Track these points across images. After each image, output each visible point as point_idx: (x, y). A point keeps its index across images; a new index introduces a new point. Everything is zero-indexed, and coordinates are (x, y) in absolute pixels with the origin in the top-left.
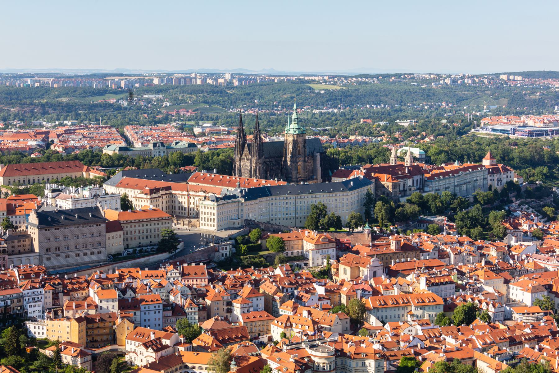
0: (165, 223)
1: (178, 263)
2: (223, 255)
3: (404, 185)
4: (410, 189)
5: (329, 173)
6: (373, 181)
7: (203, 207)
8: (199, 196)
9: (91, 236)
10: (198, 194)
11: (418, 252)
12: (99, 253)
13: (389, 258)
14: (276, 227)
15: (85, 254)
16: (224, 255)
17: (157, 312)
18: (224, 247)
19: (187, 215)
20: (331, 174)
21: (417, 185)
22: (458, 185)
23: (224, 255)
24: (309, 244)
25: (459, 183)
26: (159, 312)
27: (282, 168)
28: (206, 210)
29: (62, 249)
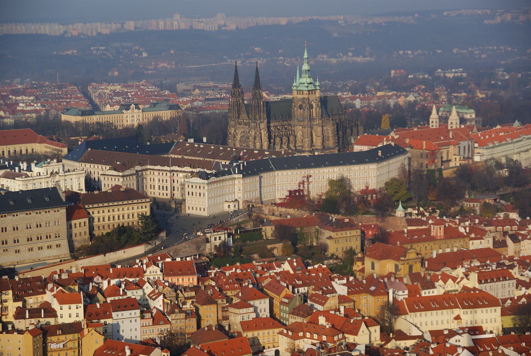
0: (142, 207)
1: (159, 258)
8: (185, 172)
9: (48, 224)
11: (467, 240)
12: (58, 246)
13: (429, 247)
15: (40, 248)
17: (133, 320)
20: (353, 141)
21: (464, 153)
22: (519, 153)
26: (136, 321)
28: (194, 190)
29: (10, 242)
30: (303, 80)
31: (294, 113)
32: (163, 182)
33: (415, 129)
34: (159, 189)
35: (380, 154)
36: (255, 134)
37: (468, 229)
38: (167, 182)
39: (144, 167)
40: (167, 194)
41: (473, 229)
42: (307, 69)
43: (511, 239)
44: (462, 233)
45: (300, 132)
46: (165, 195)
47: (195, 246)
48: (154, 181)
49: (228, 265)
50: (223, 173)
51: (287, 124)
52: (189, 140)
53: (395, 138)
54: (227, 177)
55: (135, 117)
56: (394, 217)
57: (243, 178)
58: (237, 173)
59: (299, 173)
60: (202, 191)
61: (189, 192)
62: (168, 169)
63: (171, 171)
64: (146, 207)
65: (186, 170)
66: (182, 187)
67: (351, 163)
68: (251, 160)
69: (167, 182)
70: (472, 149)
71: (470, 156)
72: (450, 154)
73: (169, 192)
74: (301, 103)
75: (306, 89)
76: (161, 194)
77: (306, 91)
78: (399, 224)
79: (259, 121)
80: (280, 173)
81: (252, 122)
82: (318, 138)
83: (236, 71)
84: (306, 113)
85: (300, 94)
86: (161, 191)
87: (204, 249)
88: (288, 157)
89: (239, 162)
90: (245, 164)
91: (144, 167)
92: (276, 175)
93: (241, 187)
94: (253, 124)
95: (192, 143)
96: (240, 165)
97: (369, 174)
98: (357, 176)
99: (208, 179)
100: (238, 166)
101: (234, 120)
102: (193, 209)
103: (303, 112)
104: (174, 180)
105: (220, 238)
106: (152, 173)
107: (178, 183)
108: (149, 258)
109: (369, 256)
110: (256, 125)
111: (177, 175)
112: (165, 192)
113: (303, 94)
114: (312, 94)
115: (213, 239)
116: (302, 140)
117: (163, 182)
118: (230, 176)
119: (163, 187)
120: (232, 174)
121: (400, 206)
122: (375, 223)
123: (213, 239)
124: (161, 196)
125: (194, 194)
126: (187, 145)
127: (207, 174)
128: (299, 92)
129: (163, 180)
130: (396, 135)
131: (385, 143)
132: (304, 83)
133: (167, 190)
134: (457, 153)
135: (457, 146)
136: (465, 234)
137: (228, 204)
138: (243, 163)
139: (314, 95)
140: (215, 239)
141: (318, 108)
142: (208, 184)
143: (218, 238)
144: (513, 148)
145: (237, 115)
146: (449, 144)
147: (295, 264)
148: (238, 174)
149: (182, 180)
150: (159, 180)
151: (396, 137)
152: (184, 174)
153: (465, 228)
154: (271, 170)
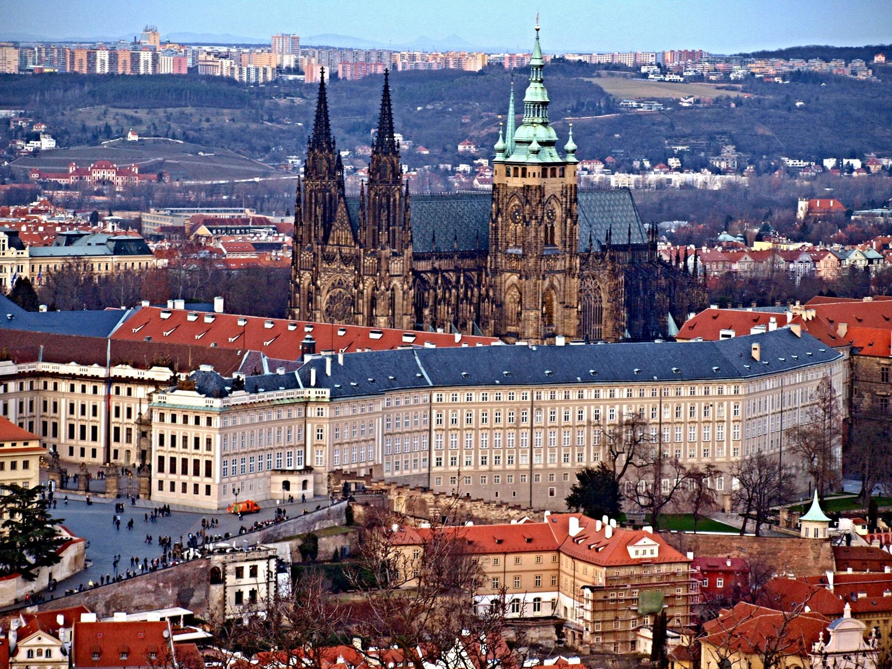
0: (14, 466)
2: (239, 595)
5: (666, 327)
6: (845, 354)
7: (168, 418)
8: (151, 382)
10: (147, 375)
14: (455, 504)
16: (246, 596)
18: (247, 567)
19: (100, 458)
23: (246, 596)
24: (580, 565)
27: (481, 298)
30: (523, 133)
31: (496, 234)
32: (83, 413)
34: (72, 436)
36: (375, 288)
38: (95, 414)
39: (27, 368)
40: (94, 452)
42: (540, 99)
45: (514, 292)
46: (88, 453)
47: (176, 590)
48: (55, 411)
50: (273, 384)
51: (473, 266)
52: (170, 304)
53: (804, 318)
54: (283, 394)
55: (8, 270)
56: (796, 540)
57: (331, 399)
58: (313, 383)
59: (505, 397)
60: (203, 433)
61: (162, 437)
62: (101, 372)
63: (109, 381)
64: (26, 465)
65: (157, 378)
66: (144, 429)
68: (359, 351)
69: (95, 414)
73: (101, 443)
74: (517, 202)
75: (534, 159)
76: (77, 452)
77: (533, 164)
78: (811, 563)
79: (388, 251)
82: (567, 311)
83: (322, 99)
84: (533, 234)
85: (516, 176)
86: (77, 443)
89: (323, 353)
90: (341, 361)
91: (27, 368)
92: (434, 400)
93: (326, 428)
94: (368, 261)
95: (179, 312)
96: (323, 361)
98: (682, 415)
99: (222, 394)
100: (320, 365)
101: (311, 249)
102: (173, 489)
103: (526, 232)
104: (117, 409)
105: (254, 572)
106: (50, 386)
107: (129, 416)
108: (28, 618)
109: (715, 642)
110: (379, 259)
111: (129, 392)
112: (88, 444)
114: (553, 175)
115: (230, 568)
116: (519, 314)
117: (83, 413)
118: (294, 393)
119: (83, 428)
120: (299, 387)
121: (816, 508)
122: (734, 554)
124: (77, 458)
125: (179, 441)
127: (226, 384)
128: (512, 168)
129: (83, 407)
130: (806, 309)
132: (530, 143)
133: (94, 438)
137: (282, 478)
138: (334, 359)
141: (569, 221)
142: (224, 412)
143: (247, 572)
145: (321, 233)
148: (316, 386)
149: (145, 408)
150: (72, 406)
151: (810, 314)
152: (152, 389)
154: (419, 384)
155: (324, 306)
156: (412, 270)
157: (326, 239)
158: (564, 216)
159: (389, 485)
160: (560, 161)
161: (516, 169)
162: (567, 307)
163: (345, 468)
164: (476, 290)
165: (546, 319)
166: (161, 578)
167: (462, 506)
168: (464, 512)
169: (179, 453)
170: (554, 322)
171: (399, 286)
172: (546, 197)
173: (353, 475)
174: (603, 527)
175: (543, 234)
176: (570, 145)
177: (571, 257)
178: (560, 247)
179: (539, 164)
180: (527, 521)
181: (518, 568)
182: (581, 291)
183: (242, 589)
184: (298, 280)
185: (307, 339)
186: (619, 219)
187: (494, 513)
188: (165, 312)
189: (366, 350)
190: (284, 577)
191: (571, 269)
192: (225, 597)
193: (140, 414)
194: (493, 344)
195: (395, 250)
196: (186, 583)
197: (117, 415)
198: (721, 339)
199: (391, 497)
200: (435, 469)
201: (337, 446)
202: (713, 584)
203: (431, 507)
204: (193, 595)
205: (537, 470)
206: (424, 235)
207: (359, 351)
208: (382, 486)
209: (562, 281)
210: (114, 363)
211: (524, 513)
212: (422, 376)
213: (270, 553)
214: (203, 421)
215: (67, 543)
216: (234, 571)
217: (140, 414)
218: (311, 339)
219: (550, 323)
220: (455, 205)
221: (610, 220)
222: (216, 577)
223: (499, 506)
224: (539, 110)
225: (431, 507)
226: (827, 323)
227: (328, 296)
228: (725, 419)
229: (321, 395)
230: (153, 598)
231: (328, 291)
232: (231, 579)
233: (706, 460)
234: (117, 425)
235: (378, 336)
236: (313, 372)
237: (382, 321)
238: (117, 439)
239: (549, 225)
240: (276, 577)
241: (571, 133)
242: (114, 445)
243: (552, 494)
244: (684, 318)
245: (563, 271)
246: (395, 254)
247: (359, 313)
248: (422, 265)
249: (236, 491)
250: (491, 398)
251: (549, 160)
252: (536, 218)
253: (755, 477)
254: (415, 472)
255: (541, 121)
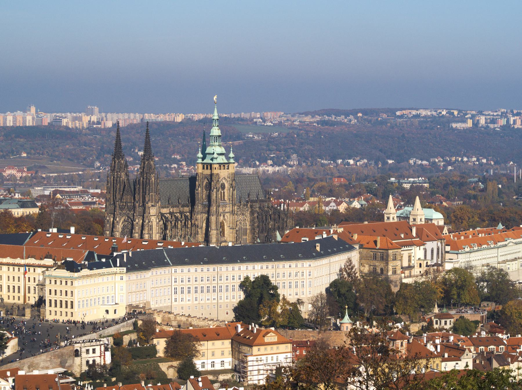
3: (410, 257)
4: (420, 264)
5: (276, 237)
11: (438, 361)
14: (184, 319)
20: (279, 238)
21: (432, 258)
22: (504, 262)
25: (504, 258)
31: (198, 196)
33: (366, 223)
35: (318, 249)
37: (439, 347)
40: (19, 297)
41: (446, 347)
42: (217, 134)
43: (497, 361)
44: (432, 353)
46: (16, 298)
47: (59, 360)
49: (105, 386)
50: (100, 266)
52: (51, 230)
53: (338, 231)
57: (127, 272)
58: (118, 265)
61: (50, 290)
63: (25, 266)
67: (278, 259)
68: (139, 250)
69: (19, 281)
70: (442, 254)
71: (440, 262)
72: (412, 258)
76: (11, 298)
79: (150, 204)
80: (179, 269)
81: (139, 206)
86: (11, 294)
87: (71, 366)
88: (190, 249)
90: (130, 255)
96: (122, 255)
97: (303, 275)
104: (29, 278)
105: (94, 351)
111: (34, 271)
112: (16, 294)
113: (211, 169)
115: (84, 350)
120: (111, 267)
123: (84, 350)
125: (58, 293)
126: (49, 235)
130: (339, 228)
131: (325, 236)
133: (19, 292)
134: (422, 257)
135: (422, 247)
136: (435, 353)
138: (128, 254)
139: (226, 170)
140: (88, 351)
143: (91, 351)
144: (496, 255)
146: (412, 244)
147: (201, 384)
149: (41, 278)
151: (340, 230)
153: (436, 348)
154: (165, 264)
155: (120, 230)
156: (160, 213)
157: (121, 199)
158: (229, 187)
159: (154, 310)
160: (227, 162)
161: (207, 166)
162: (231, 228)
163: (133, 303)
164: (189, 221)
165: (222, 234)
166: (52, 354)
167: (187, 320)
168: (187, 322)
169: (58, 298)
170: (225, 236)
171: (155, 220)
172: (221, 179)
173: (137, 307)
174: (252, 328)
175: (220, 196)
176: (232, 155)
177: (233, 205)
178: (228, 201)
179: (218, 164)
180: (217, 326)
181: (213, 347)
182: (237, 221)
183: (89, 359)
184: (108, 218)
185: (114, 245)
186: (253, 188)
187: (202, 323)
188: (49, 234)
189: (142, 250)
190: (108, 354)
191: (232, 211)
192: (81, 363)
193: (39, 280)
194: (200, 246)
195: (153, 204)
196: (64, 357)
197: (29, 281)
198: (302, 242)
199: (155, 316)
200: (174, 303)
201: (130, 294)
202: (301, 352)
203: (173, 320)
204: (67, 362)
205: (220, 303)
206: (165, 197)
207: (139, 250)
208: (150, 311)
209: (229, 217)
210: (28, 257)
211: (215, 322)
212: (168, 261)
213: (101, 343)
214: (69, 283)
215: (9, 339)
216: (85, 351)
217: (39, 280)
218: (116, 245)
219: (224, 236)
220: (179, 183)
221: (249, 188)
222: (77, 353)
223: (204, 320)
224: (217, 139)
225: (173, 320)
226: (348, 234)
227: (122, 225)
228: (305, 278)
229: (122, 271)
230: (49, 364)
231: (122, 223)
232: (84, 355)
233: (297, 297)
234: (29, 286)
235: (146, 243)
236: (118, 260)
237: (146, 237)
238: (29, 292)
239: (222, 191)
240: (104, 353)
241: (231, 149)
242: (27, 295)
243: (227, 314)
244: (284, 232)
245: (229, 212)
246: (152, 206)
247: (137, 233)
248: (165, 211)
249: (85, 315)
250: (199, 270)
251: (222, 162)
252: (216, 188)
253: (320, 304)
254: (165, 305)
255: (218, 144)
